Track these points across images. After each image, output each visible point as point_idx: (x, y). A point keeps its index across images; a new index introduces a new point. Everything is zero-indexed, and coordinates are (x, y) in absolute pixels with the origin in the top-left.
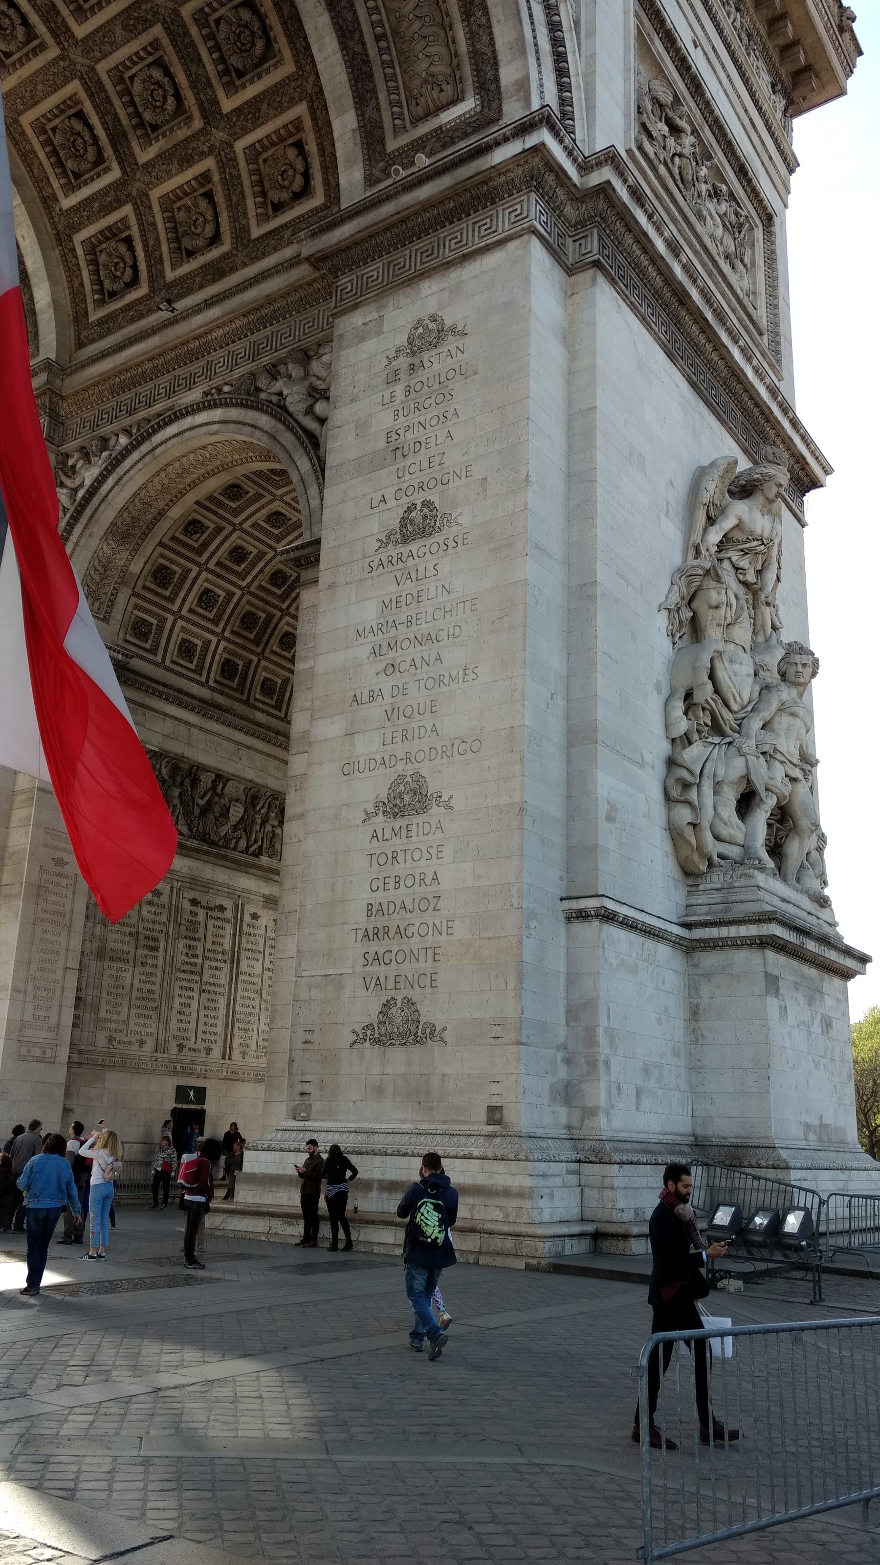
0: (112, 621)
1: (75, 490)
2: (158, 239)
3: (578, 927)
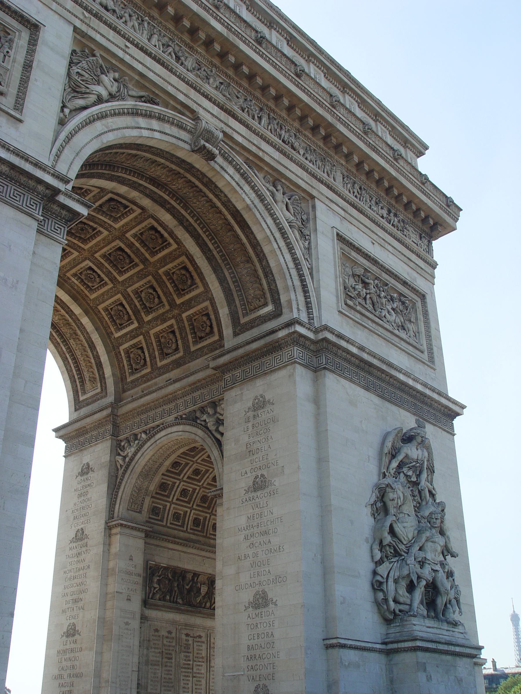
0: (143, 512)
1: (125, 457)
2: (154, 349)
3: (330, 651)
